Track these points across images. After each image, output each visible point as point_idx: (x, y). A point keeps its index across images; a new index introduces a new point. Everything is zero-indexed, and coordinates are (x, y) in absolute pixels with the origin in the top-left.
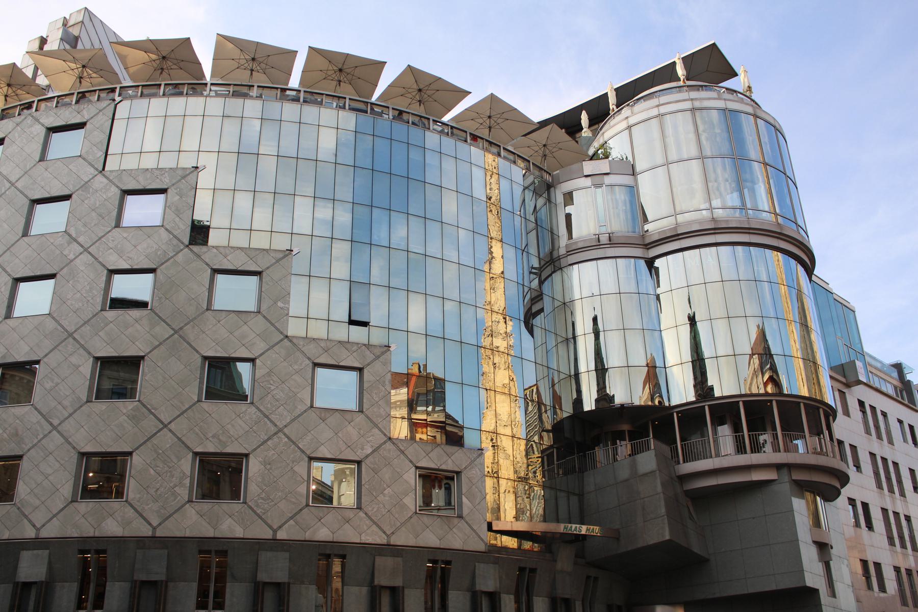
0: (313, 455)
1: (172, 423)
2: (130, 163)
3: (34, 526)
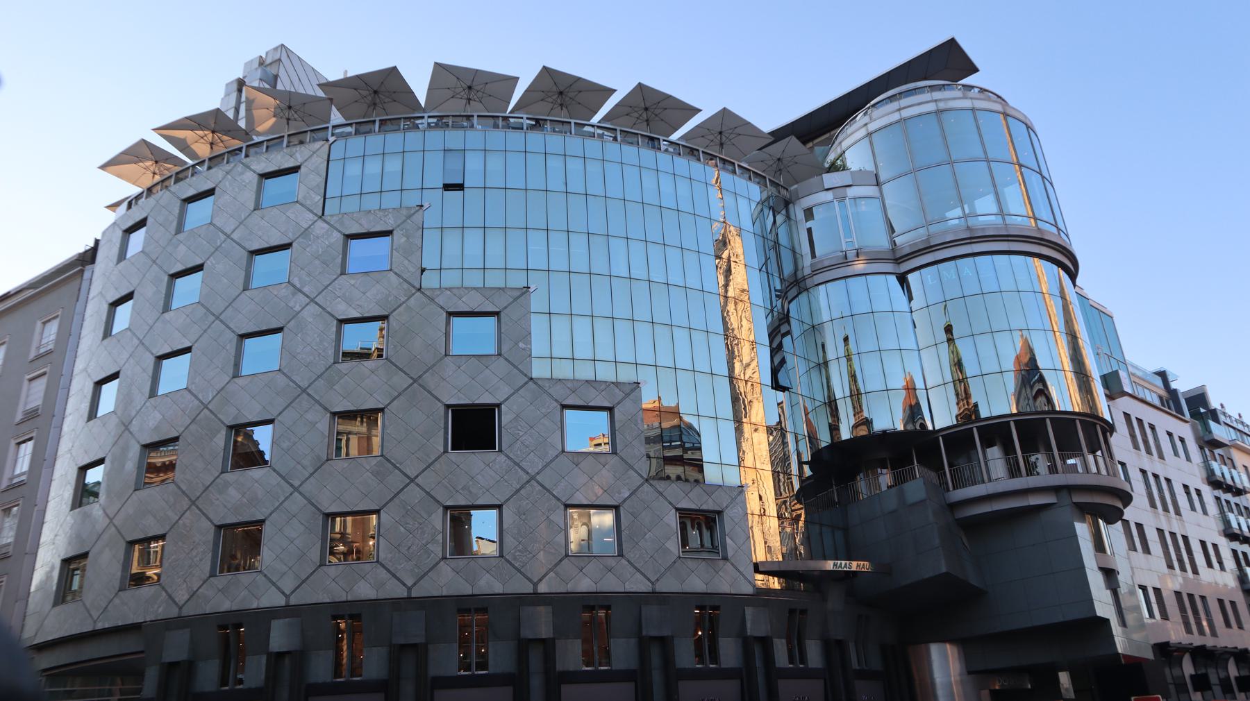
0: (569, 502)
1: (419, 477)
2: (351, 205)
3: (283, 593)
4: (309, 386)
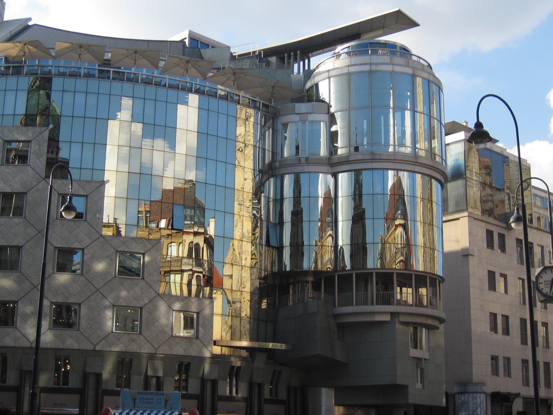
0: (116, 304)
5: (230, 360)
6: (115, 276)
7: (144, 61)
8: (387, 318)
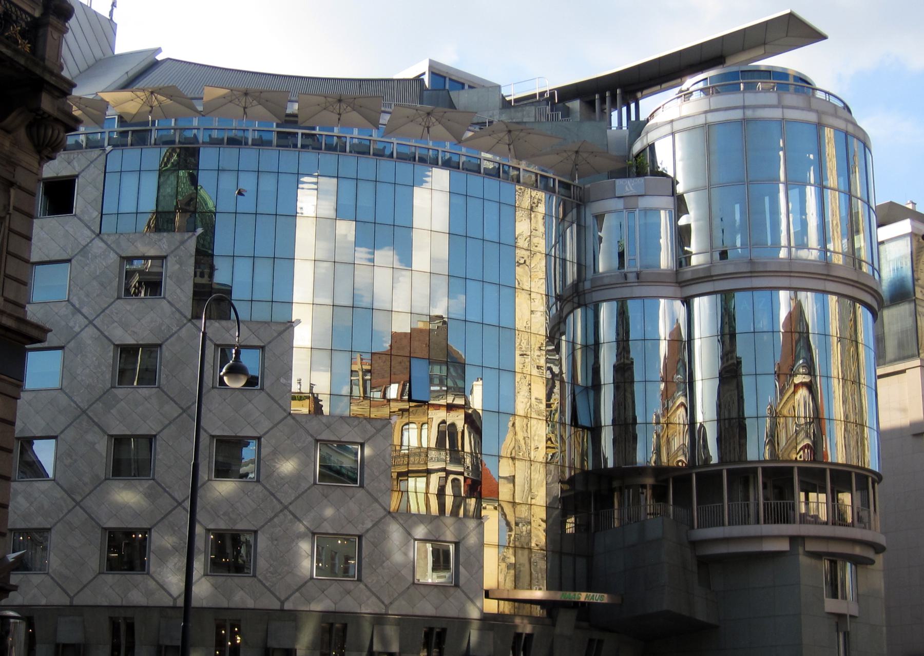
4: (88, 408)
5: (513, 622)
6: (315, 483)
7: (355, 116)
8: (784, 546)
